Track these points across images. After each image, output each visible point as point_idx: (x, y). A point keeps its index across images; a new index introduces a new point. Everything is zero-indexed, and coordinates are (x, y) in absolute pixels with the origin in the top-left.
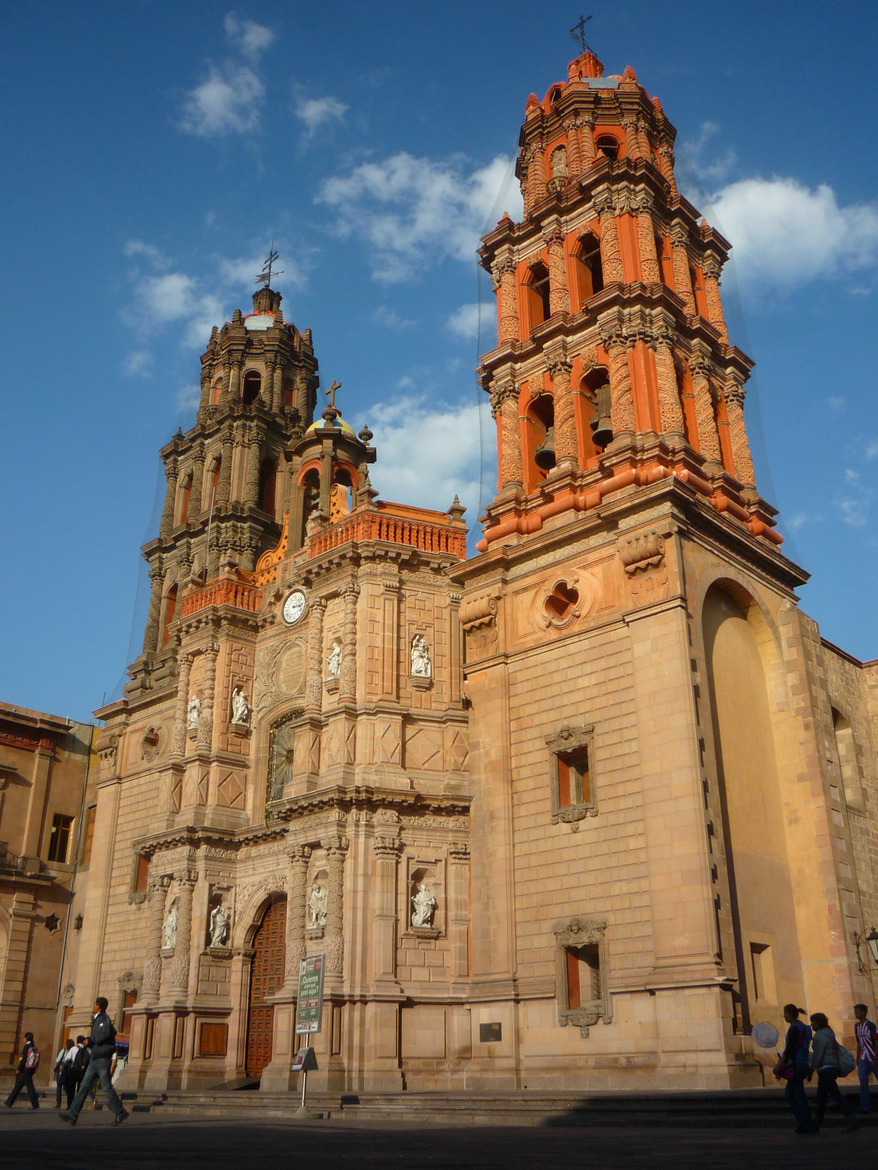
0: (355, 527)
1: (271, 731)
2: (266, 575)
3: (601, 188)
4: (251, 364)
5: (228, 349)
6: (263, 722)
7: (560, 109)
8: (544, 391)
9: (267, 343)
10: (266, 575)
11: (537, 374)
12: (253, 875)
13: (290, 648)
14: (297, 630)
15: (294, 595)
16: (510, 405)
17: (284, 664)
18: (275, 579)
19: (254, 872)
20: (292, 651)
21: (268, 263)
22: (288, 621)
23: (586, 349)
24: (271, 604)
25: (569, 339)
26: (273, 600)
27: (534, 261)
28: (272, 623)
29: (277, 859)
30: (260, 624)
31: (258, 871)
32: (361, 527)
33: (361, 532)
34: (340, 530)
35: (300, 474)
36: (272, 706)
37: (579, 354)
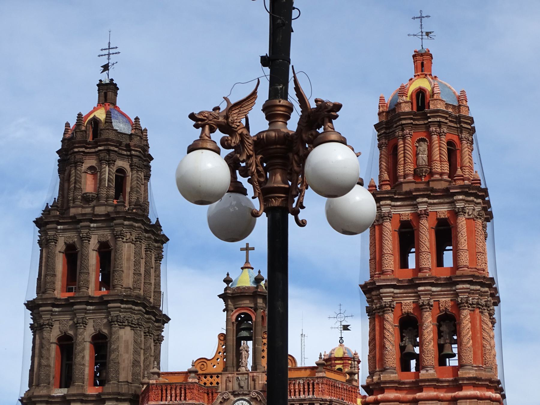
0: (315, 384)
2: (208, 377)
3: (461, 197)
4: (120, 163)
5: (106, 148)
7: (428, 115)
8: (412, 314)
9: (133, 148)
10: (208, 377)
11: (409, 301)
15: (241, 401)
16: (390, 316)
18: (218, 383)
21: (106, 52)
23: (444, 300)
25: (434, 289)
27: (405, 218)
32: (320, 387)
33: (320, 389)
34: (302, 382)
35: (235, 313)
37: (439, 301)
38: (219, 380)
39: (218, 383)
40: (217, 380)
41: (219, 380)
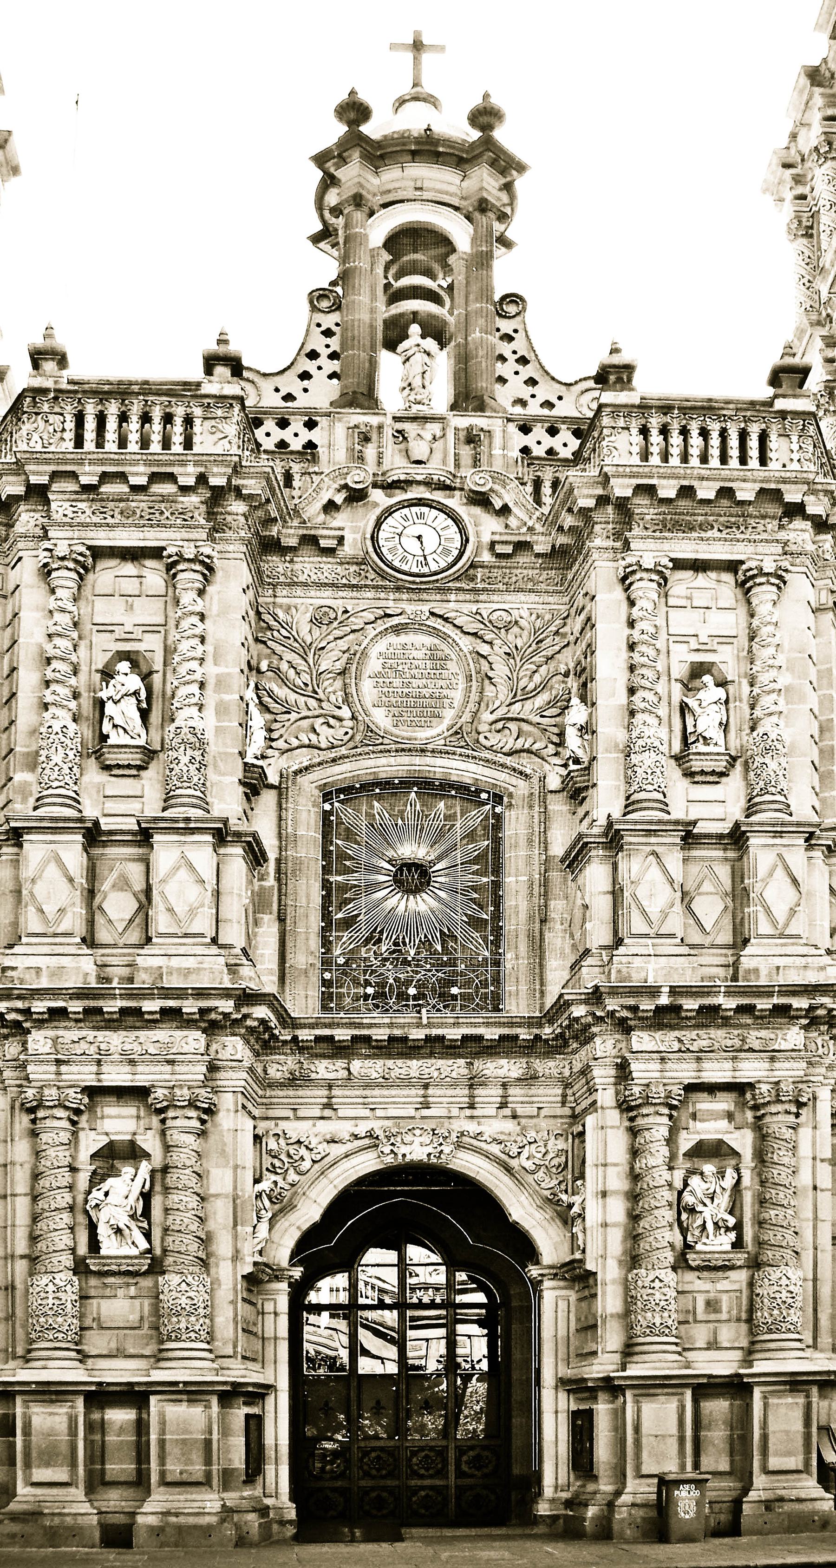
1: (327, 807)
6: (304, 780)
12: (322, 1118)
13: (397, 630)
14: (425, 596)
17: (374, 664)
19: (327, 1113)
20: (403, 638)
22: (396, 563)
24: (330, 507)
26: (339, 499)
28: (330, 552)
29: (424, 1097)
30: (293, 542)
31: (341, 1113)
36: (343, 751)
38: (315, 436)
39: (310, 445)
40: (306, 435)
41: (315, 436)
